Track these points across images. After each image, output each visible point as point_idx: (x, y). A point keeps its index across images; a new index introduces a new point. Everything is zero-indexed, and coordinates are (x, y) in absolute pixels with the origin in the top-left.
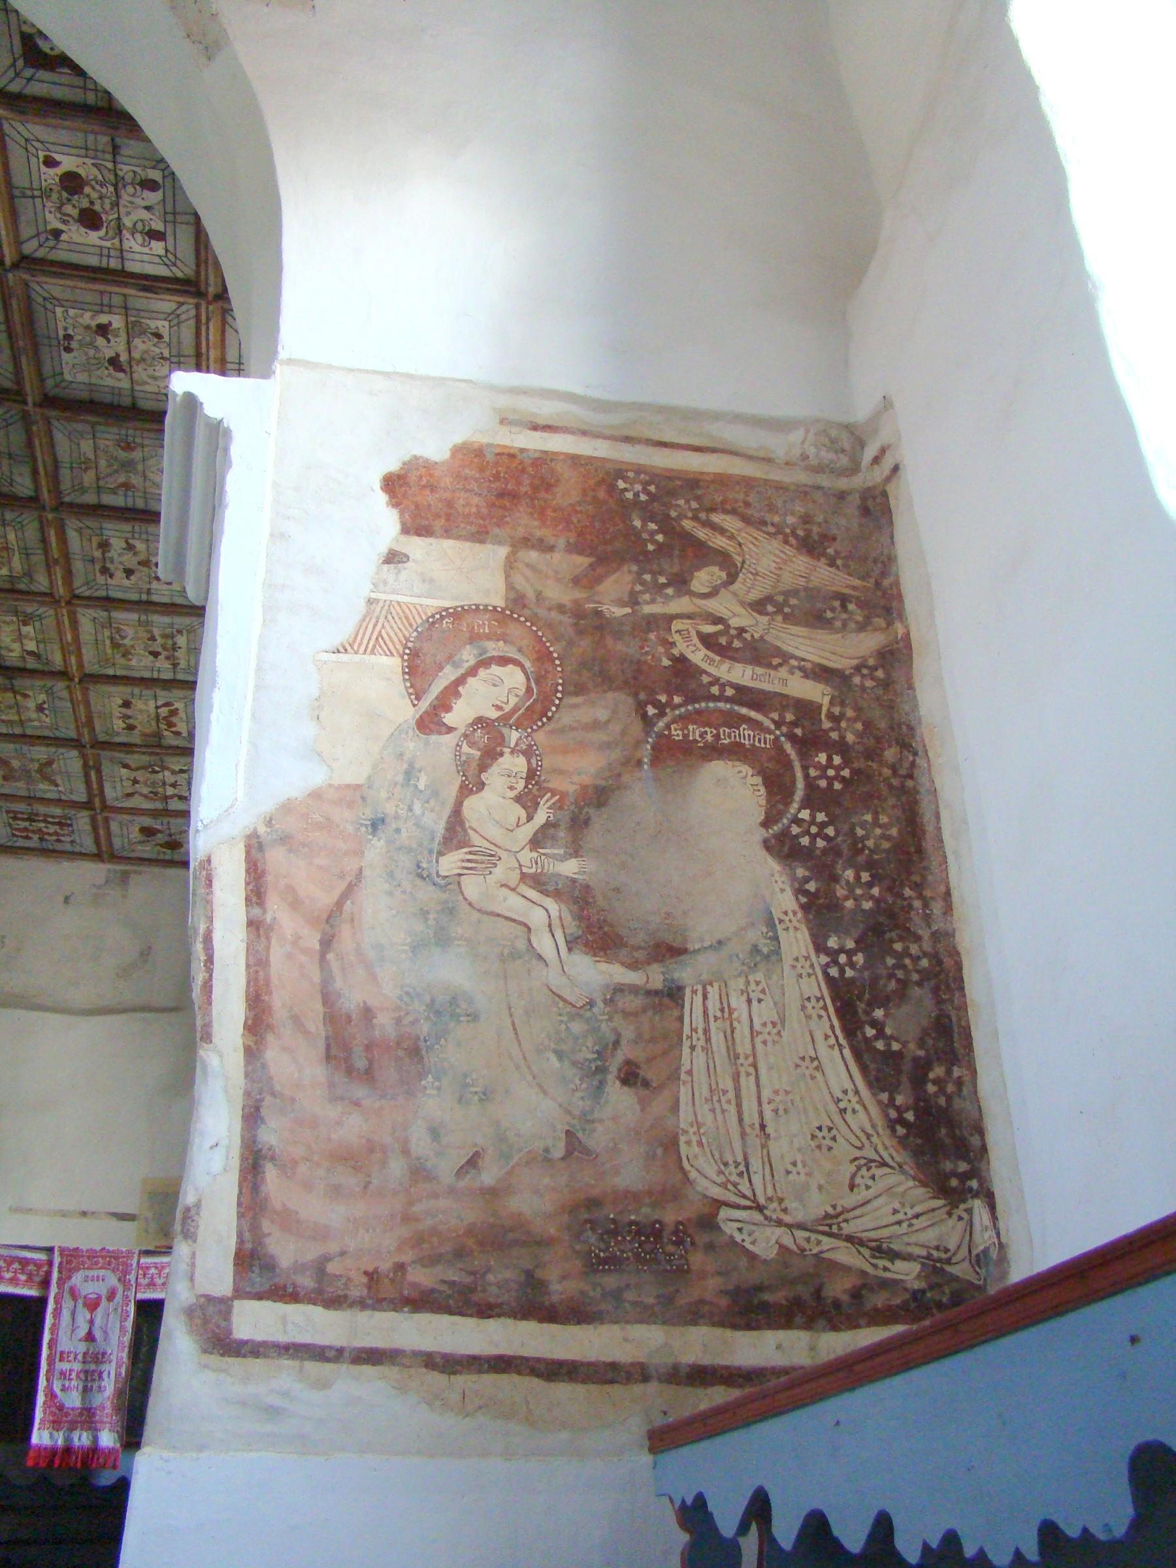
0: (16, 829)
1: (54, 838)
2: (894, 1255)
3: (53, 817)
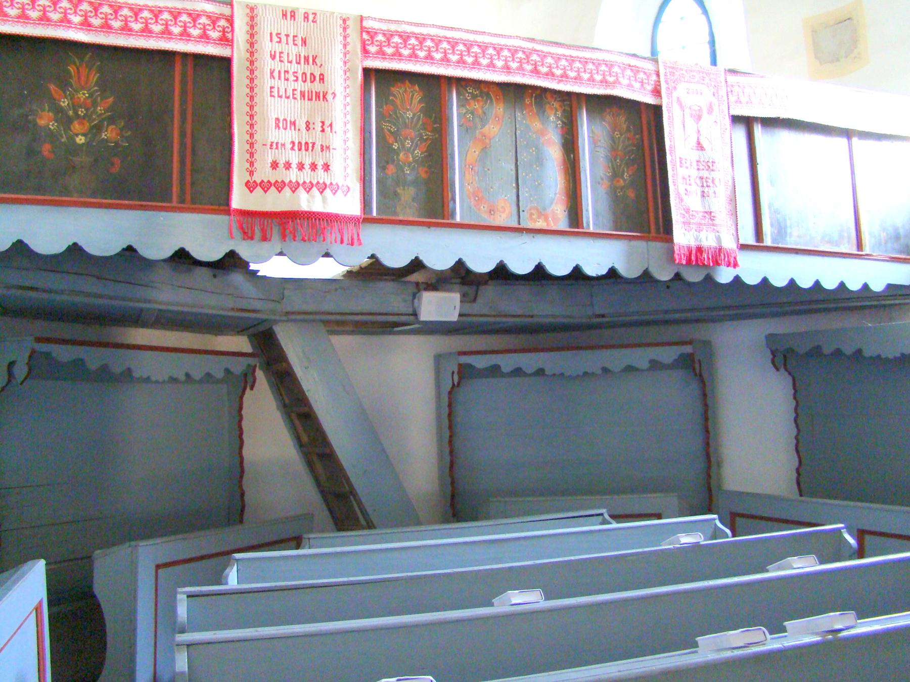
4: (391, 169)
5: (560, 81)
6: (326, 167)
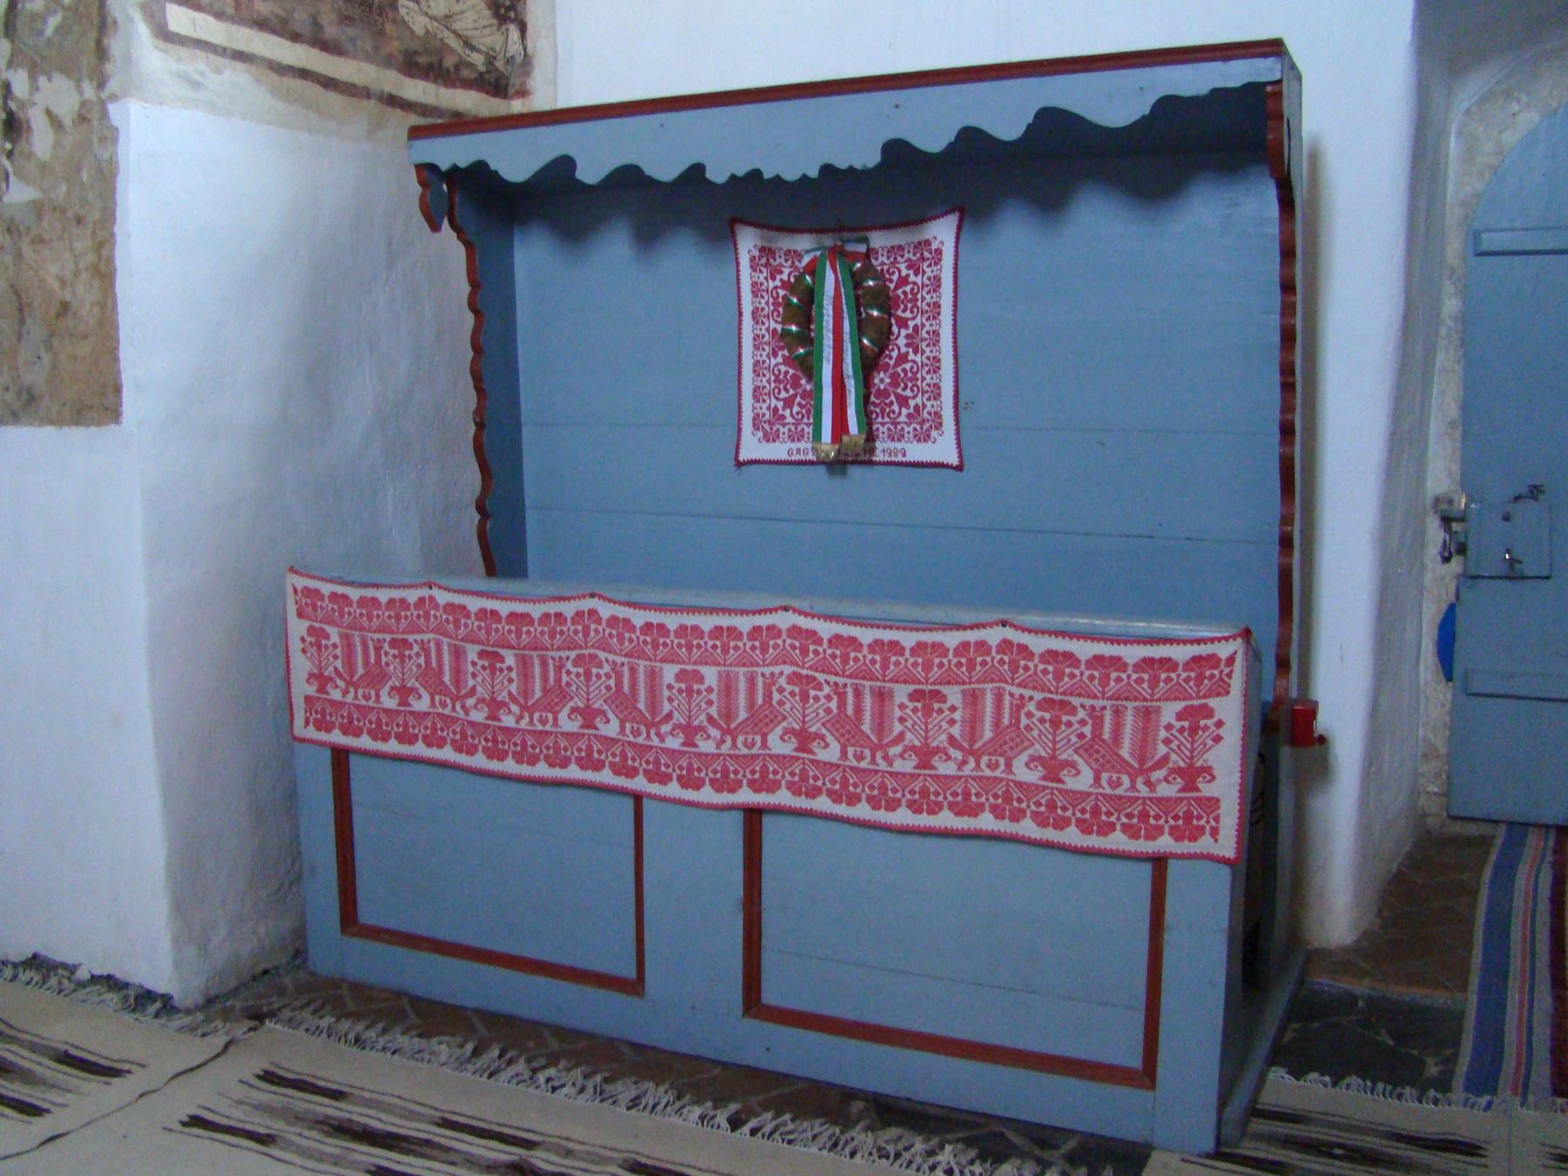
2: (473, 48)
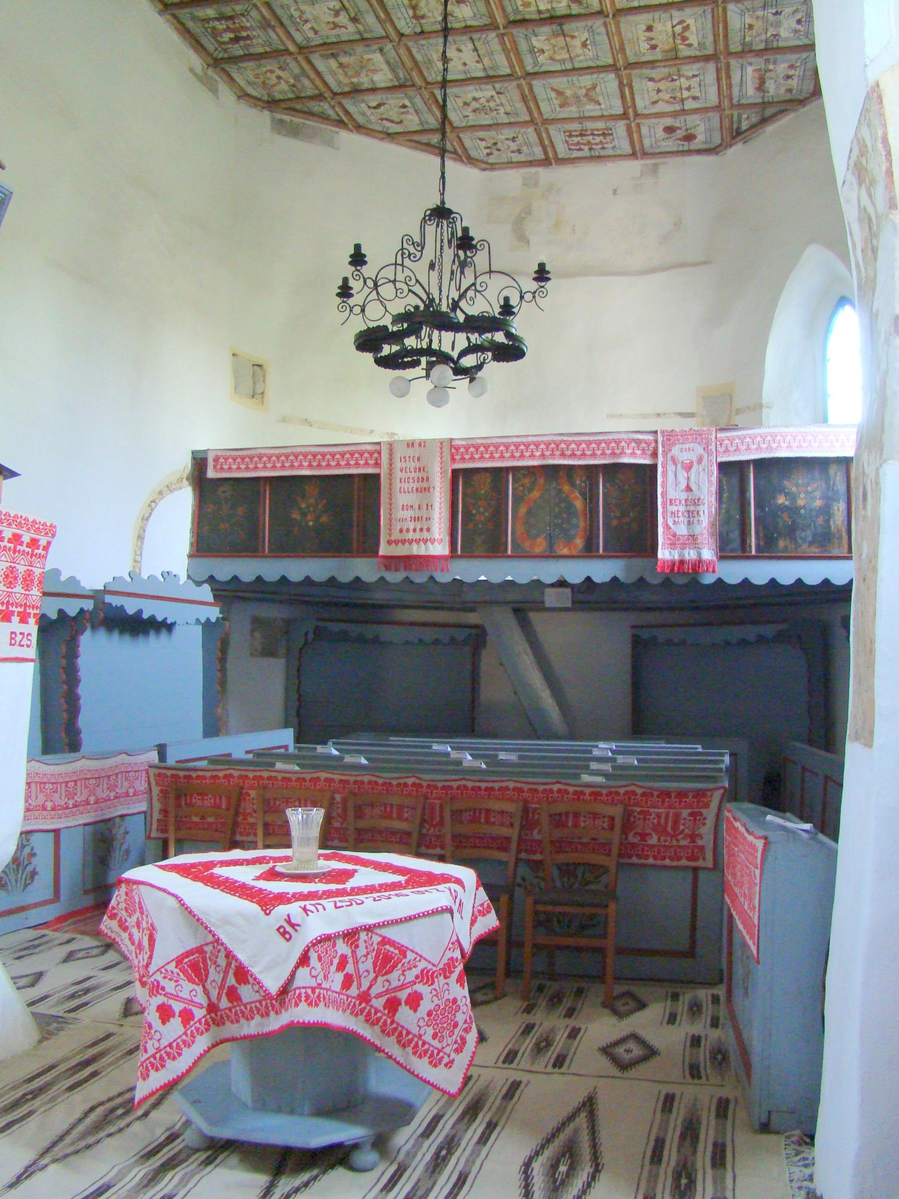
0: (573, 144)
1: (600, 146)
3: (598, 130)
4: (471, 526)
5: (580, 459)
6: (428, 530)
